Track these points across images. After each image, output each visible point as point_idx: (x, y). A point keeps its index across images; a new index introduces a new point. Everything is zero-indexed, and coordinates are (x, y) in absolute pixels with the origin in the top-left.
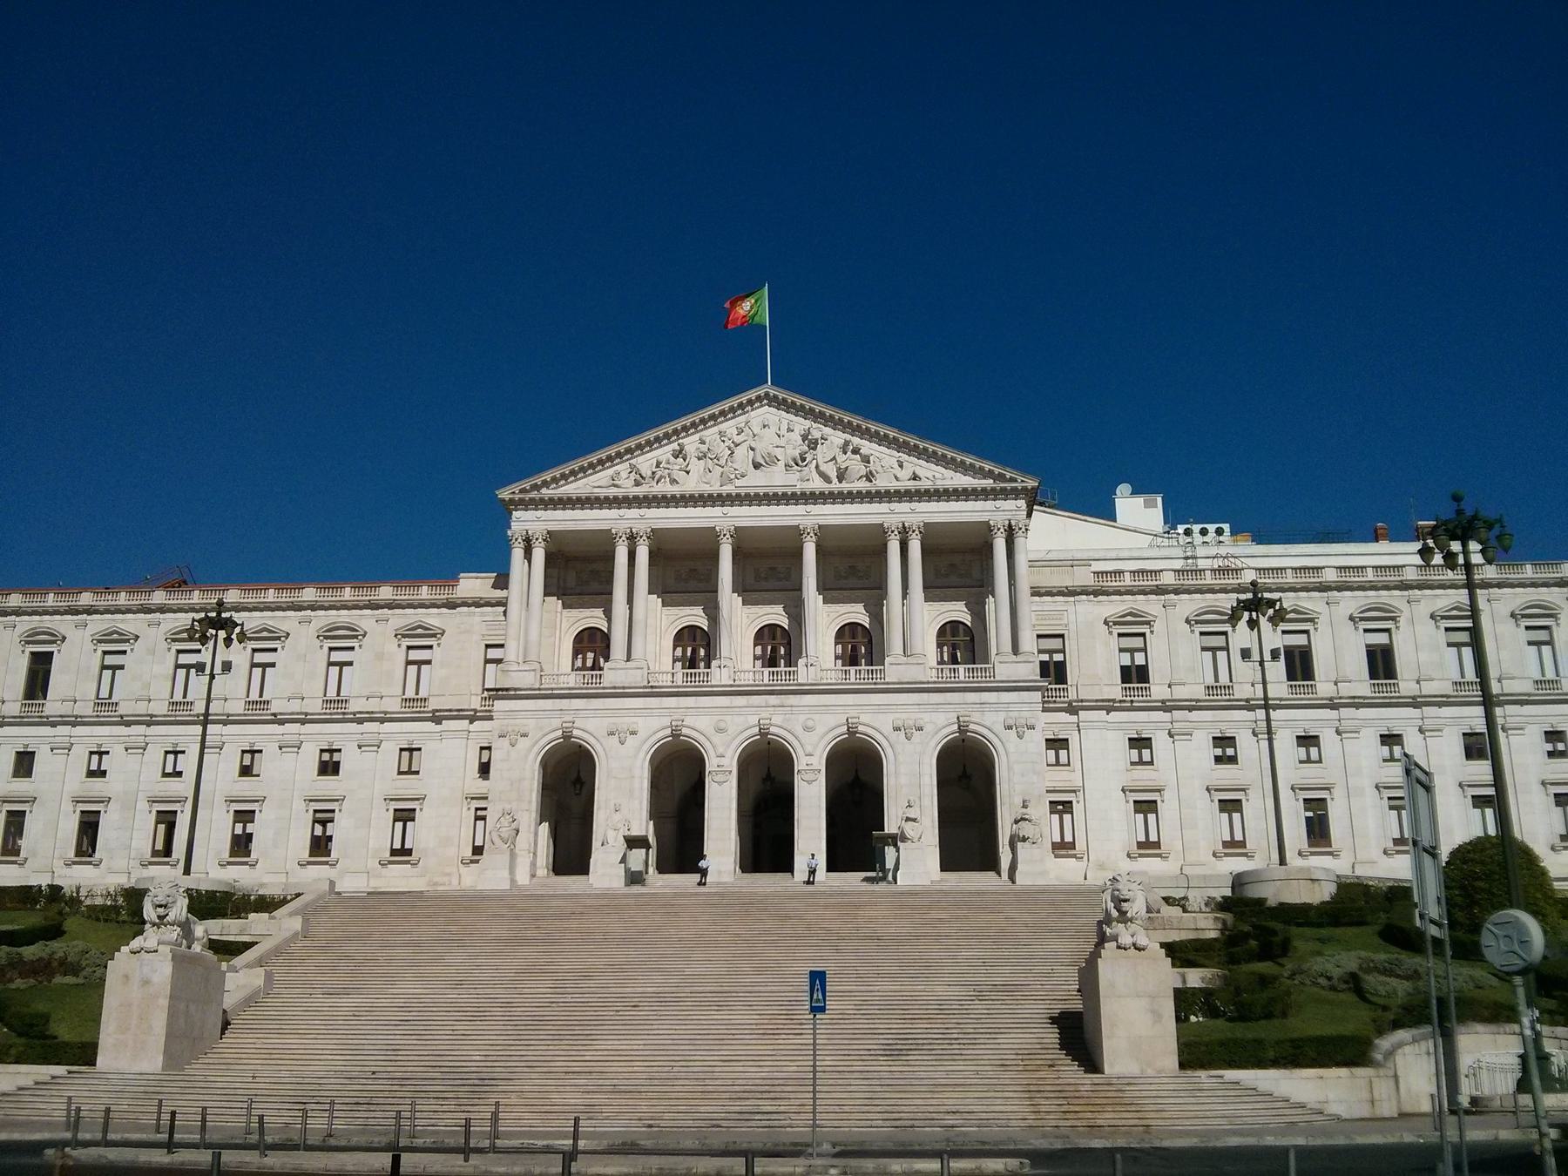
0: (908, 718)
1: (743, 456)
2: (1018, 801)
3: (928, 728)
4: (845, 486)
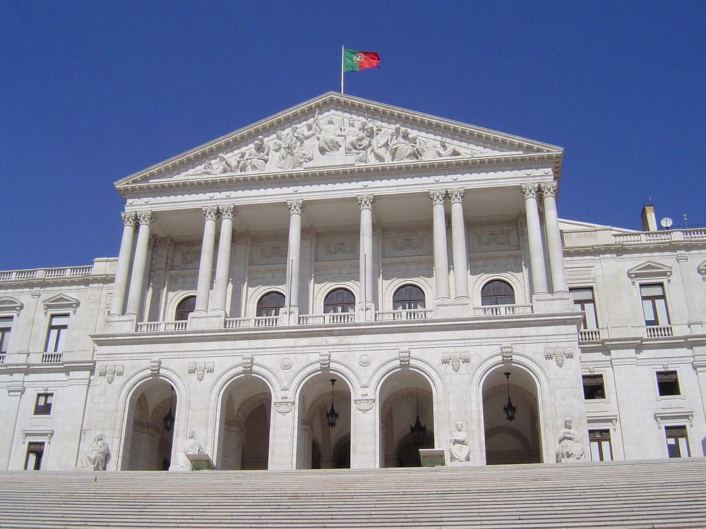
0: (452, 352)
1: (311, 146)
2: (560, 422)
3: (474, 361)
4: (397, 163)
